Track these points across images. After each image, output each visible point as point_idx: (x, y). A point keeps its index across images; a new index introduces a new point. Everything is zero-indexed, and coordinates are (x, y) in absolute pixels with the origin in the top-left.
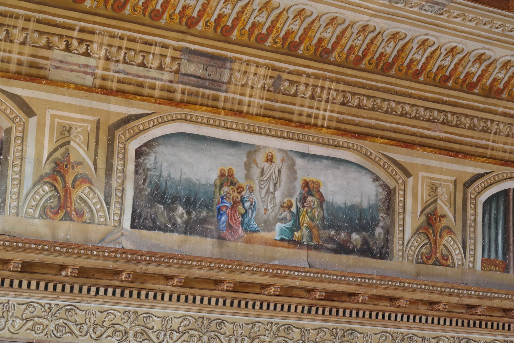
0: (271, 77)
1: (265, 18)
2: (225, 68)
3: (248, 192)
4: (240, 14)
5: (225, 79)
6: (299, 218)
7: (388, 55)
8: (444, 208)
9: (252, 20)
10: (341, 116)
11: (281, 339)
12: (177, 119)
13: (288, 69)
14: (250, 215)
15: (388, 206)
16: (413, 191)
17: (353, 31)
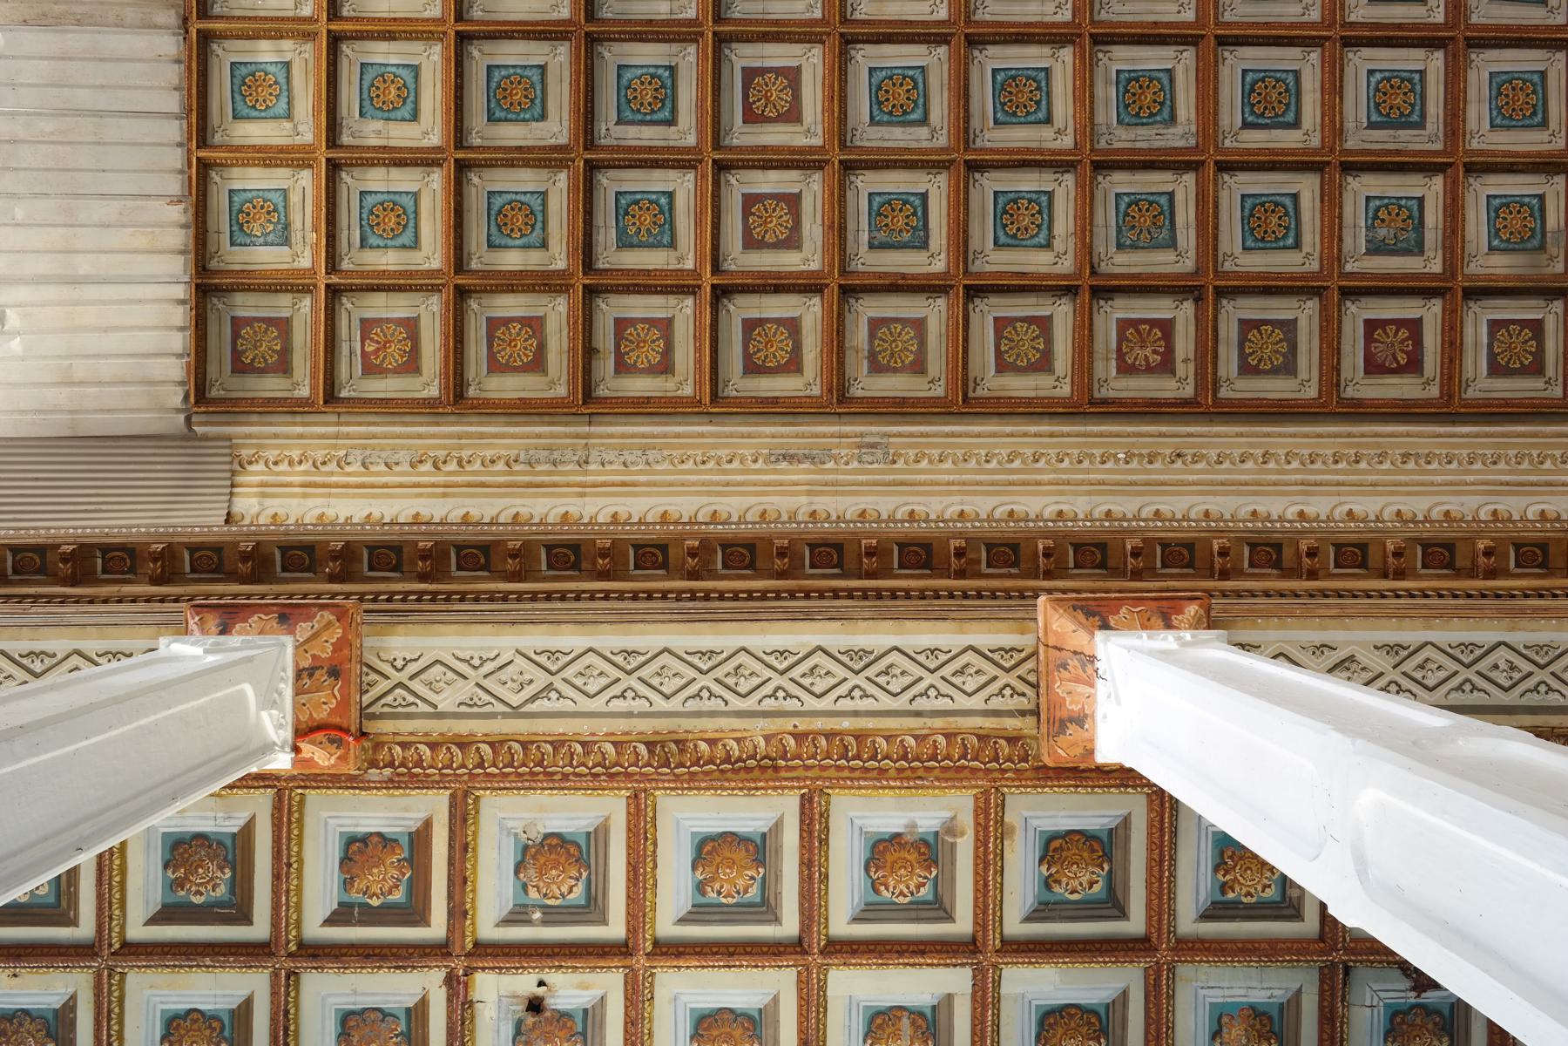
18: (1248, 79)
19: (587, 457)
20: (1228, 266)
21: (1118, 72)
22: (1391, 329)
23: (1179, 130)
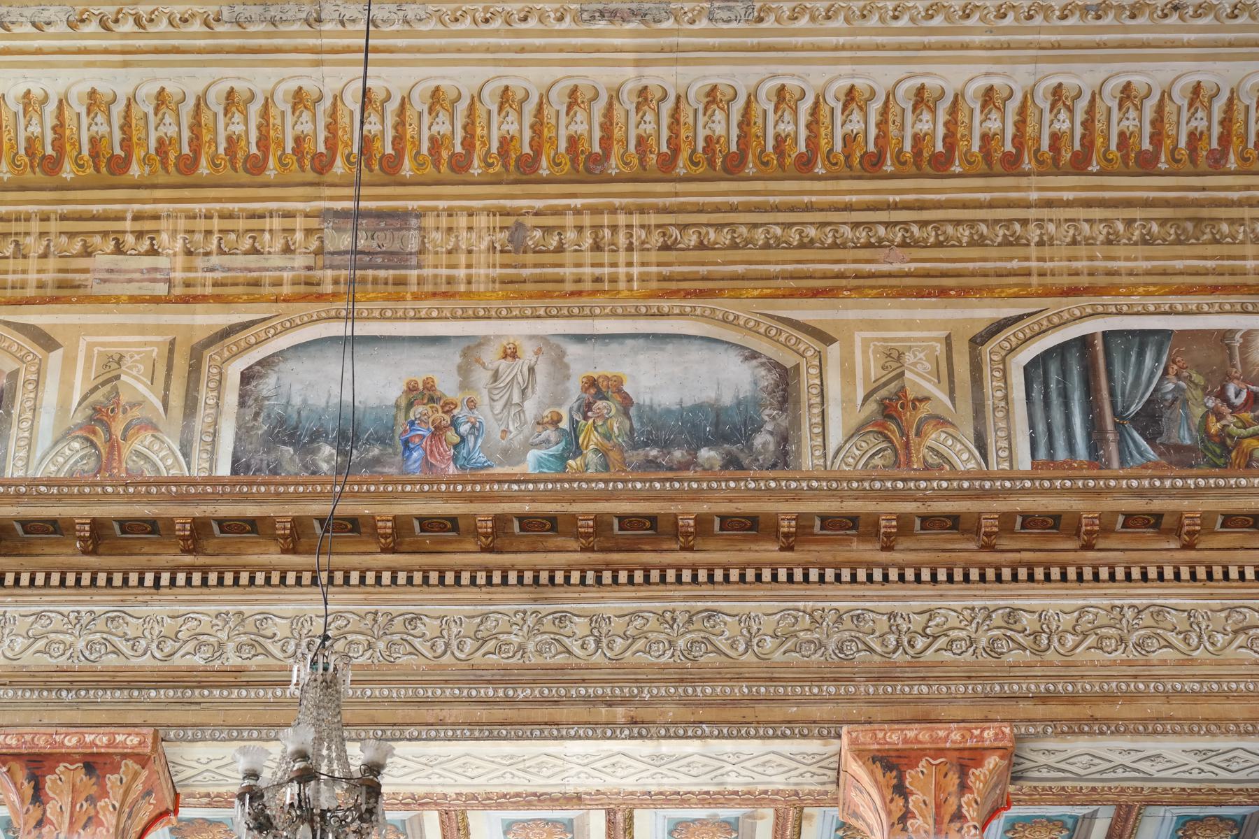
0: (502, 228)
1: (447, 123)
2: (409, 229)
3: (466, 409)
4: (400, 128)
5: (413, 245)
6: (577, 438)
7: (722, 140)
8: (920, 380)
9: (426, 135)
10: (665, 270)
11: (545, 636)
12: (320, 319)
13: (533, 208)
14: (471, 445)
15: (783, 396)
16: (842, 365)
17: (628, 107)
19: (319, 13)
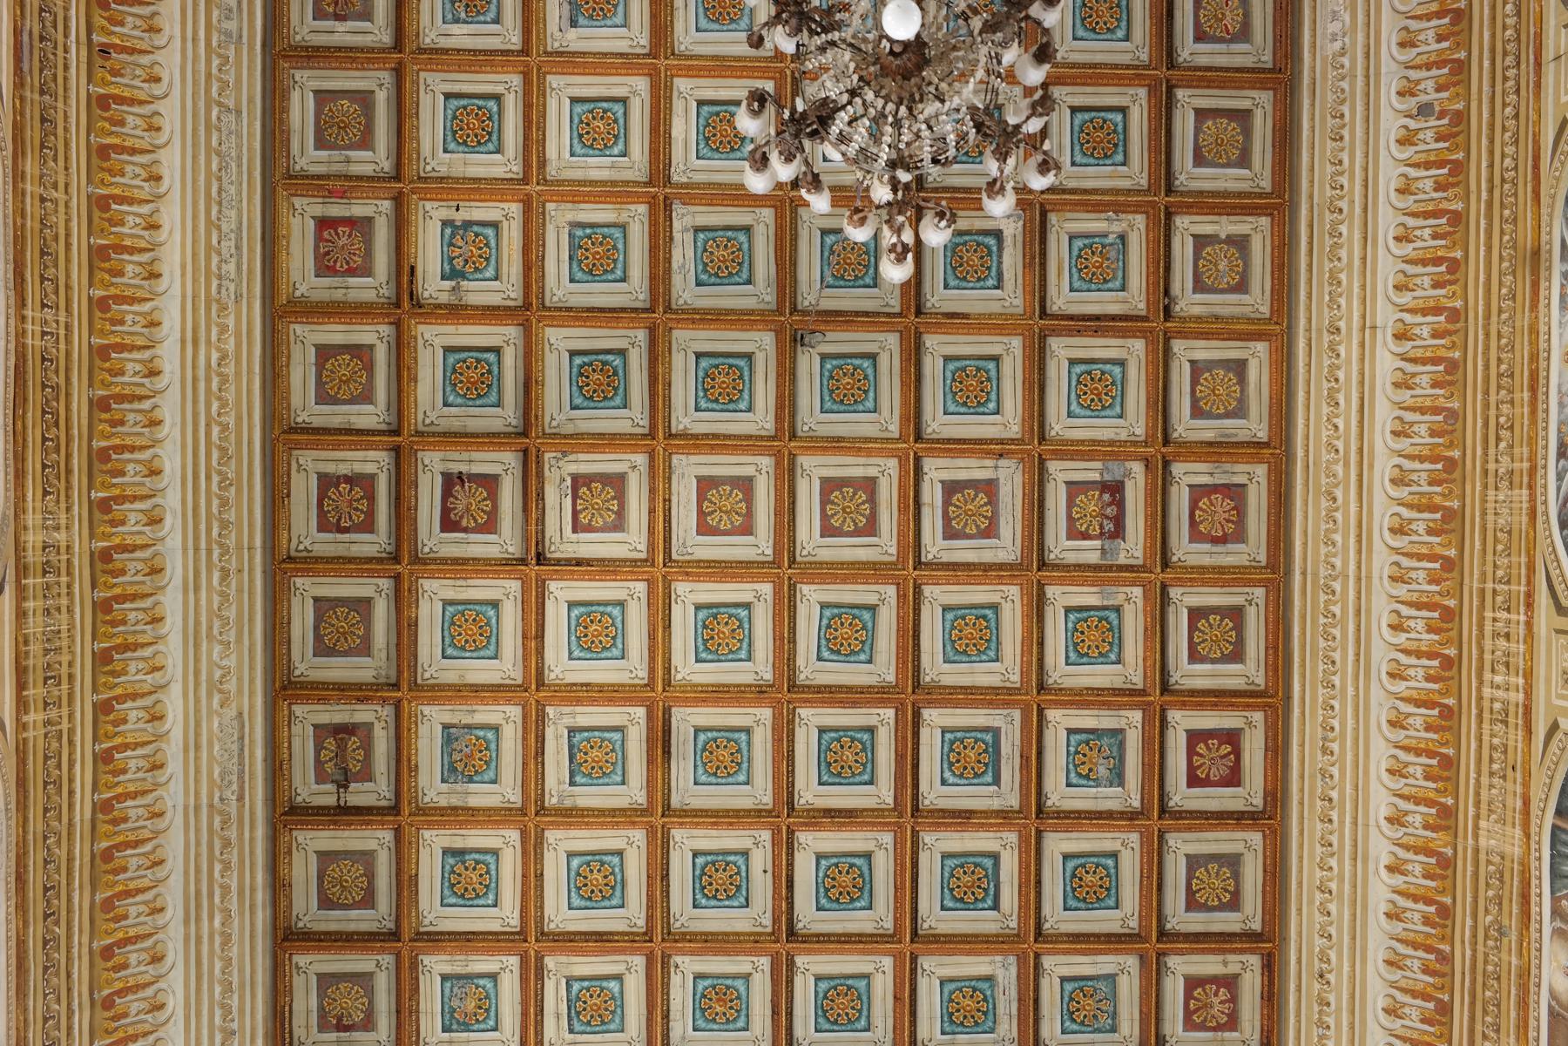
18: (950, 904)
20: (1134, 924)
21: (943, 1033)
22: (1197, 761)
23: (1000, 974)
